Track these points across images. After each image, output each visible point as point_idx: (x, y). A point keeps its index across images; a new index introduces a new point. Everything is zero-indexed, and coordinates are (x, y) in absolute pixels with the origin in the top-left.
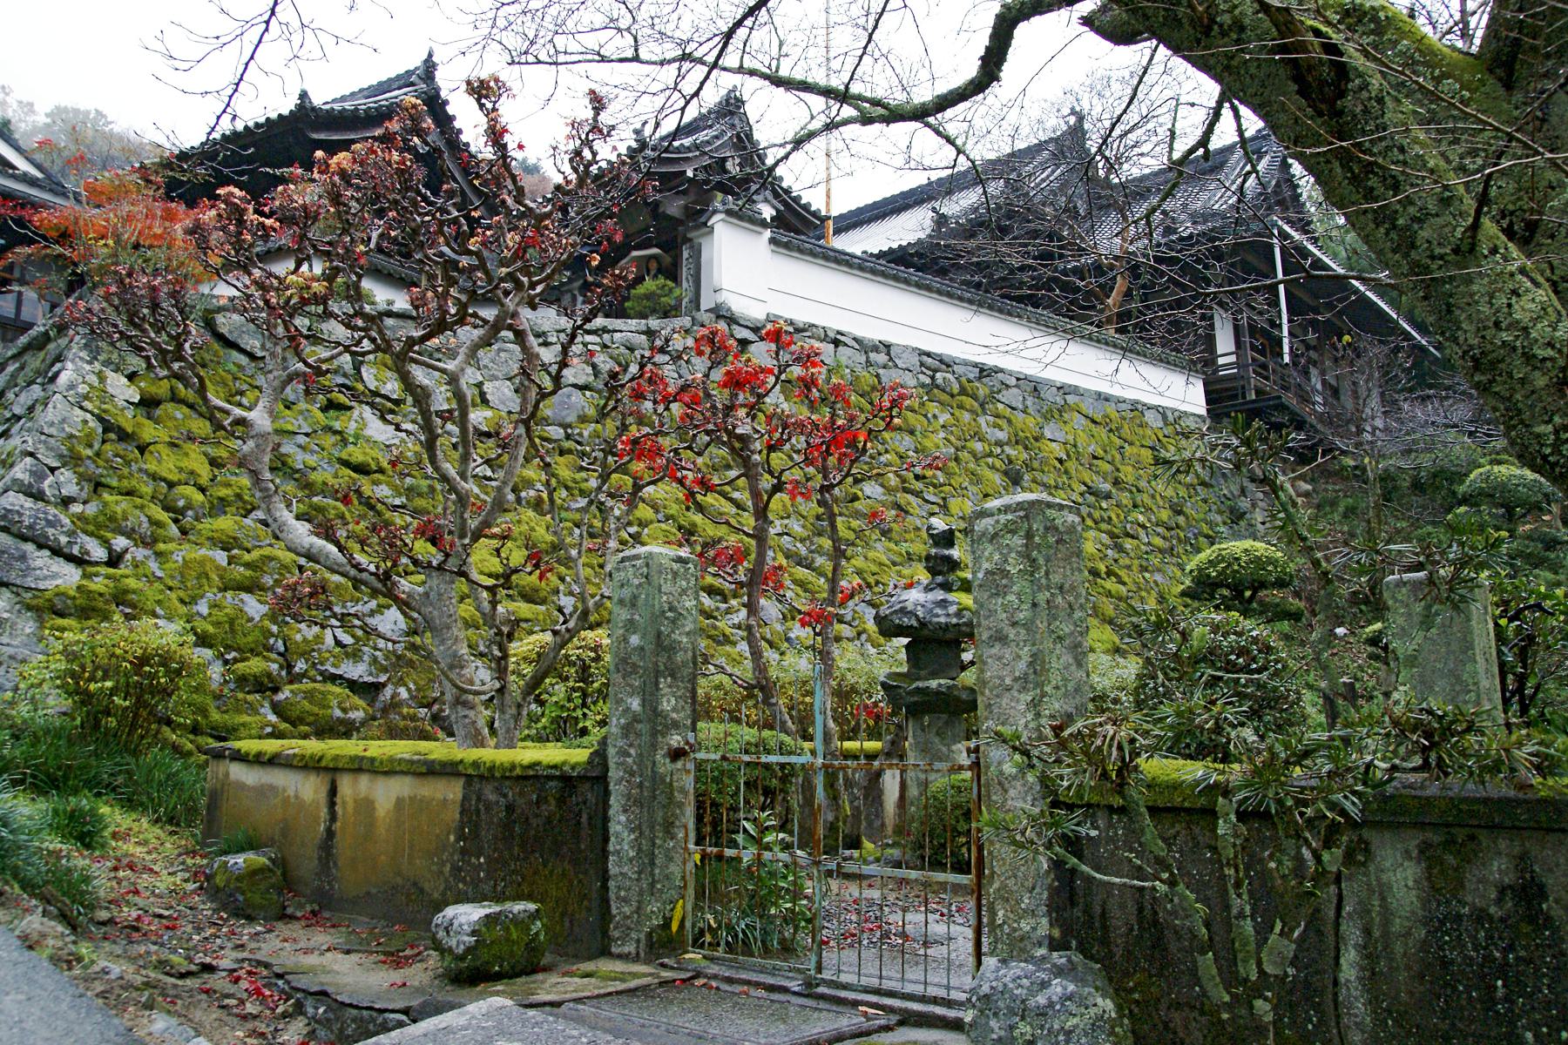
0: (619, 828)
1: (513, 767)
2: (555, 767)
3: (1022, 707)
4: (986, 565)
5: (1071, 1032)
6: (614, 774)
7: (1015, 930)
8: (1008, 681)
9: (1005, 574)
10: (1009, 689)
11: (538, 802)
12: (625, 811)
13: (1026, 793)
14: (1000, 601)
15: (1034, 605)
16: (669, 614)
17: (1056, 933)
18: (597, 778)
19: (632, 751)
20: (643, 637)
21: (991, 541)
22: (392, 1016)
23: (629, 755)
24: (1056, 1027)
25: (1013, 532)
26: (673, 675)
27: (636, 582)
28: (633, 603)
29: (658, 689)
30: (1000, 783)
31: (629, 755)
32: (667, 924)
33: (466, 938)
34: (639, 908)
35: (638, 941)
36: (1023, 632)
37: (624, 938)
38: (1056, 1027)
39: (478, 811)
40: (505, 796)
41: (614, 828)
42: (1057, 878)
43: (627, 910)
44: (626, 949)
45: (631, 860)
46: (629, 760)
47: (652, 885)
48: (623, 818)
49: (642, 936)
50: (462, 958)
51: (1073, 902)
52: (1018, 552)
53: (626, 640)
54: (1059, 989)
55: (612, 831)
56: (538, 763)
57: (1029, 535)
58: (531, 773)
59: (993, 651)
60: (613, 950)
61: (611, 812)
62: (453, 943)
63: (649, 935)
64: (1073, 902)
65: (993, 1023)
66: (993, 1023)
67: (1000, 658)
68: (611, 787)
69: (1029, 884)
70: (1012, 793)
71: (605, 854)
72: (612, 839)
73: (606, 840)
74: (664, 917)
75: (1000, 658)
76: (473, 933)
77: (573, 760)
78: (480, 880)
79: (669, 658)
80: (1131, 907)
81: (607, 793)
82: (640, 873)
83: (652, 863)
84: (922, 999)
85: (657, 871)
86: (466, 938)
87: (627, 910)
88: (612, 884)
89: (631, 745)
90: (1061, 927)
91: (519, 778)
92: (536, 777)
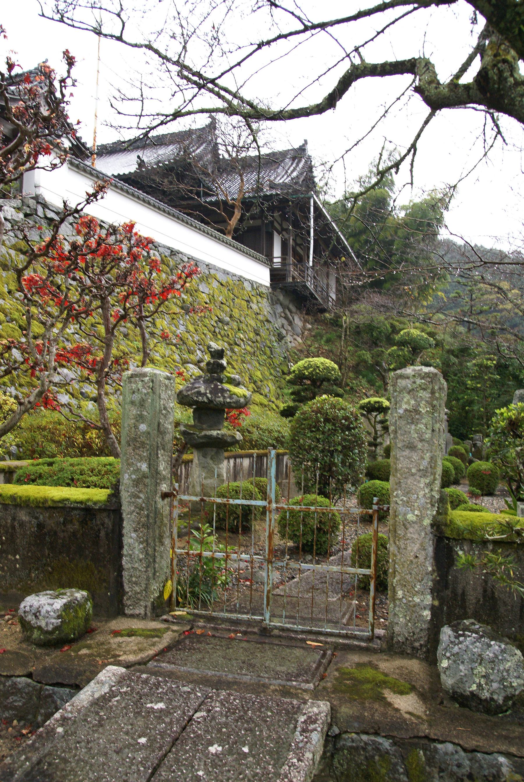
0: (131, 541)
1: (45, 500)
2: (81, 502)
3: (422, 485)
4: (404, 406)
5: (509, 670)
6: (126, 508)
7: (410, 601)
8: (414, 471)
9: (417, 411)
10: (413, 475)
11: (64, 524)
12: (135, 531)
13: (421, 531)
14: (413, 427)
15: (433, 431)
16: (164, 412)
17: (436, 603)
18: (114, 511)
19: (141, 495)
20: (149, 426)
21: (409, 393)
22: (19, 679)
23: (139, 497)
24: (501, 668)
25: (424, 389)
26: (164, 449)
27: (144, 391)
28: (142, 404)
29: (158, 458)
30: (404, 525)
31: (139, 497)
32: (162, 593)
33: (53, 621)
34: (146, 588)
35: (146, 607)
36: (426, 445)
37: (136, 604)
38: (501, 668)
39: (13, 527)
40: (36, 518)
41: (126, 540)
42: (439, 575)
43: (137, 589)
44: (137, 612)
45: (141, 560)
46: (140, 501)
47: (154, 574)
48: (134, 535)
49: (149, 604)
50: (51, 633)
51: (446, 587)
52: (426, 401)
53: (136, 427)
54: (497, 647)
55: (125, 542)
56: (67, 500)
57: (433, 393)
58: (61, 505)
59: (404, 453)
60: (126, 612)
61: (124, 531)
62: (43, 624)
63: (153, 603)
64: (446, 587)
65: (461, 667)
66: (461, 667)
67: (409, 458)
68: (124, 515)
69: (420, 577)
70: (411, 530)
71: (120, 556)
72: (125, 547)
73: (121, 547)
74: (160, 591)
75: (409, 458)
76: (59, 617)
77: (96, 498)
78: (17, 570)
79: (163, 438)
80: (480, 590)
81: (121, 520)
82: (147, 567)
83: (154, 561)
84: (346, 636)
85: (157, 566)
86: (53, 621)
87: (137, 589)
88: (125, 574)
89: (140, 491)
90: (439, 600)
91: (50, 507)
92: (63, 508)
